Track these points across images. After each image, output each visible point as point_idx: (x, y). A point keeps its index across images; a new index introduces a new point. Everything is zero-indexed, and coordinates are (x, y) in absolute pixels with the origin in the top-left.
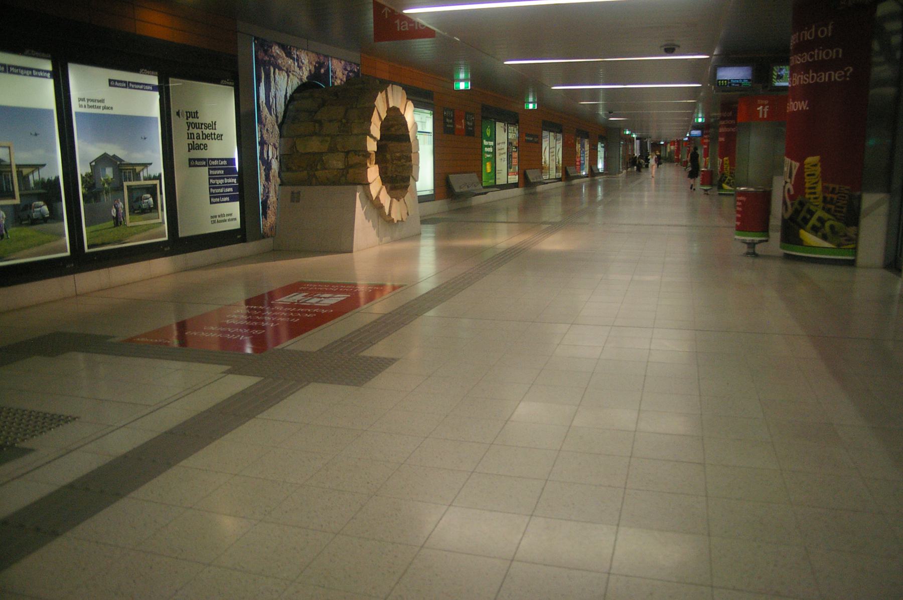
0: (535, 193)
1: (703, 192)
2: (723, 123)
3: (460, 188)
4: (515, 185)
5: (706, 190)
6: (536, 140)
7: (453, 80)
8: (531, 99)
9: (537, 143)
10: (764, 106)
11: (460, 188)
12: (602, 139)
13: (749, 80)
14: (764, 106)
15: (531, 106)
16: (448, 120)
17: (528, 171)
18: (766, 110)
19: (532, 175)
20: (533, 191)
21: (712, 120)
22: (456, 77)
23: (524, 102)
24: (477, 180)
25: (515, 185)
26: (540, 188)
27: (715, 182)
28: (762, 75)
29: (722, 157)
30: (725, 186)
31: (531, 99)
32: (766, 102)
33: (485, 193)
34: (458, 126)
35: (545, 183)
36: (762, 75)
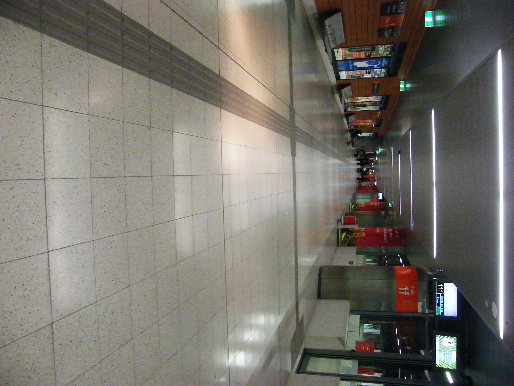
0: (333, 93)
1: (339, 218)
2: (390, 230)
3: (330, 26)
4: (338, 78)
5: (341, 220)
6: (375, 91)
7: (434, 9)
8: (408, 86)
9: (373, 92)
10: (409, 291)
11: (330, 26)
12: (376, 135)
13: (443, 313)
14: (409, 291)
15: (402, 86)
16: (394, 7)
17: (350, 86)
18: (406, 293)
19: (347, 90)
20: (335, 91)
21: (390, 212)
22: (438, 12)
23: (406, 81)
24: (338, 43)
25: (338, 78)
26: (337, 96)
27: (347, 226)
28: (447, 326)
29: (364, 232)
30: (344, 235)
31: (408, 86)
32: (412, 293)
33: (326, 51)
34: (388, 19)
35: (341, 101)
36: (447, 326)
